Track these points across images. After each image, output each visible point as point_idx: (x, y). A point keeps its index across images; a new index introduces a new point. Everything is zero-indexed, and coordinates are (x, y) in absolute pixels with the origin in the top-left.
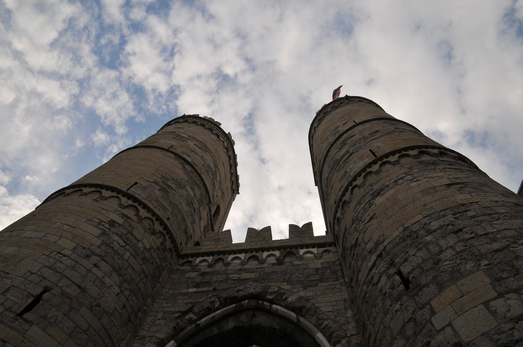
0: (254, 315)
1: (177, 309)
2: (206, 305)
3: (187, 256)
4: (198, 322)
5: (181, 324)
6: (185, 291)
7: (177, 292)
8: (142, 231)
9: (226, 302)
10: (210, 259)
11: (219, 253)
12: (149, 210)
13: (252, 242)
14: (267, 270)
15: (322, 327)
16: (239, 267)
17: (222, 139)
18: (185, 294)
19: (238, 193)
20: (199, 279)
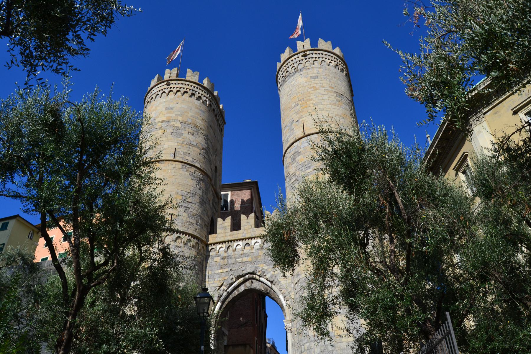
0: (252, 282)
1: (216, 285)
2: (230, 281)
3: (211, 244)
4: (228, 291)
5: (221, 293)
6: (217, 272)
7: (213, 272)
8: (188, 251)
9: (238, 277)
10: (224, 246)
11: (228, 241)
12: (186, 234)
13: (245, 230)
14: (255, 255)
15: (282, 292)
16: (241, 252)
17: (205, 98)
18: (218, 274)
19: (225, 123)
20: (222, 262)
